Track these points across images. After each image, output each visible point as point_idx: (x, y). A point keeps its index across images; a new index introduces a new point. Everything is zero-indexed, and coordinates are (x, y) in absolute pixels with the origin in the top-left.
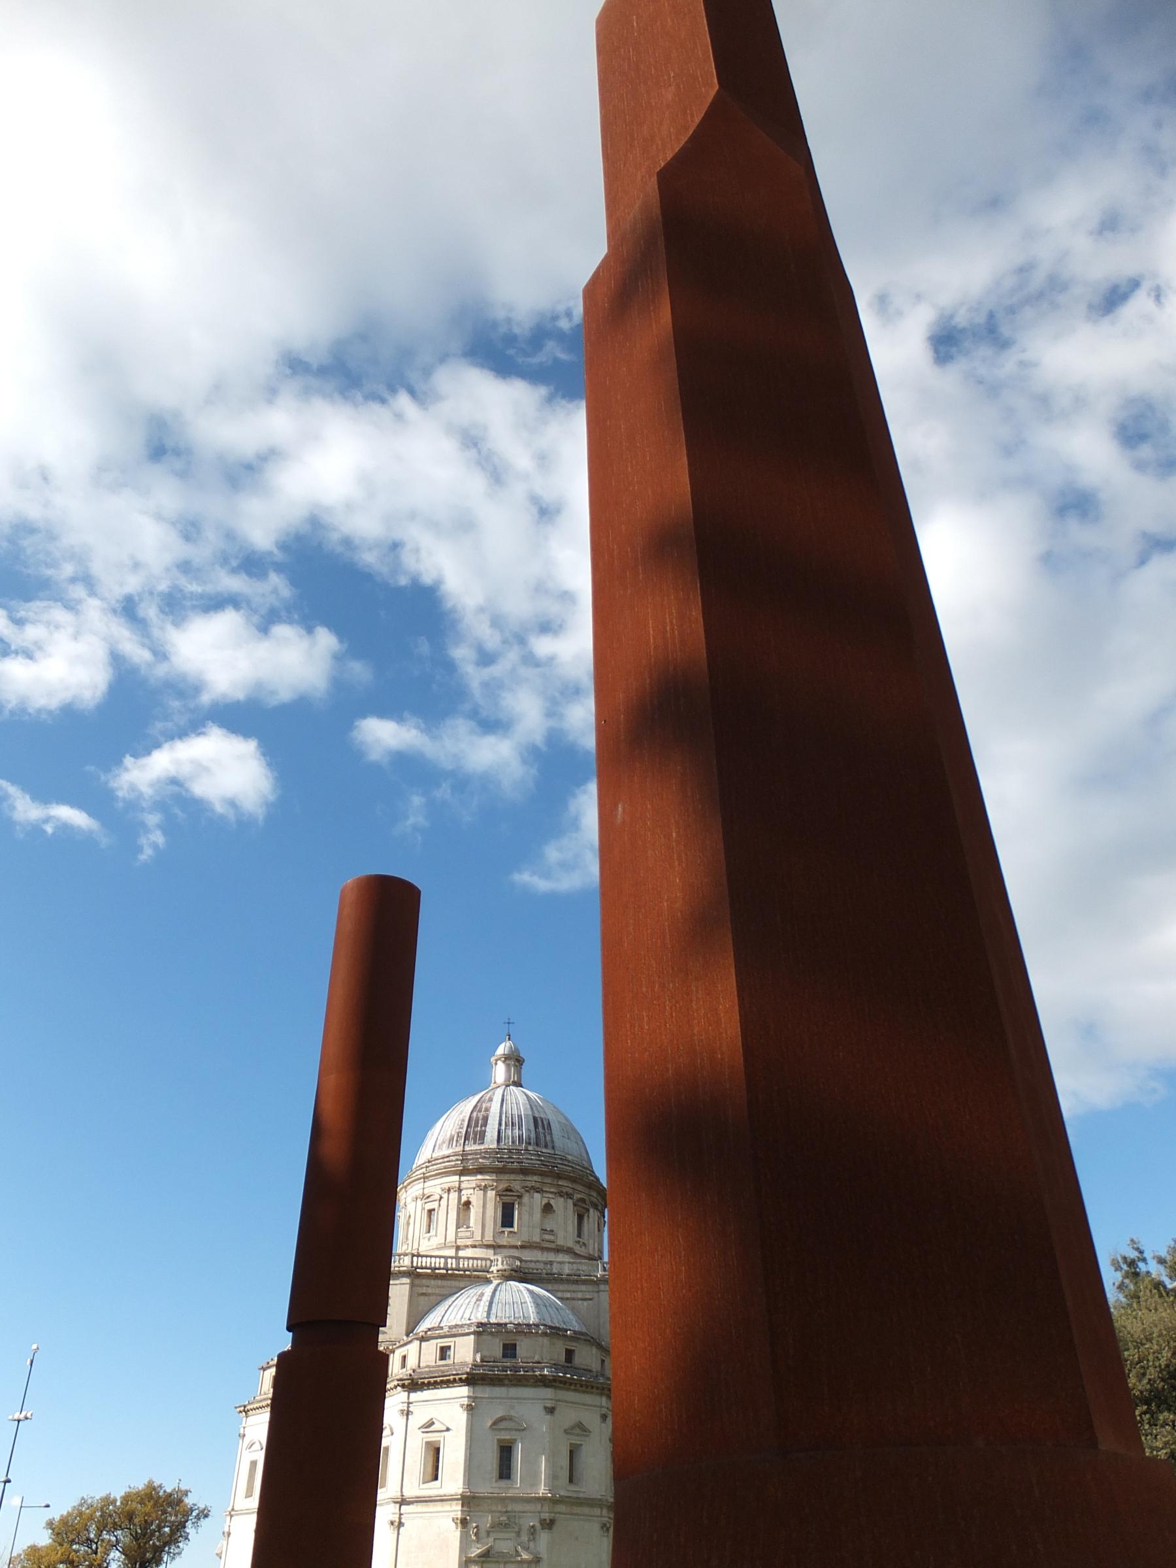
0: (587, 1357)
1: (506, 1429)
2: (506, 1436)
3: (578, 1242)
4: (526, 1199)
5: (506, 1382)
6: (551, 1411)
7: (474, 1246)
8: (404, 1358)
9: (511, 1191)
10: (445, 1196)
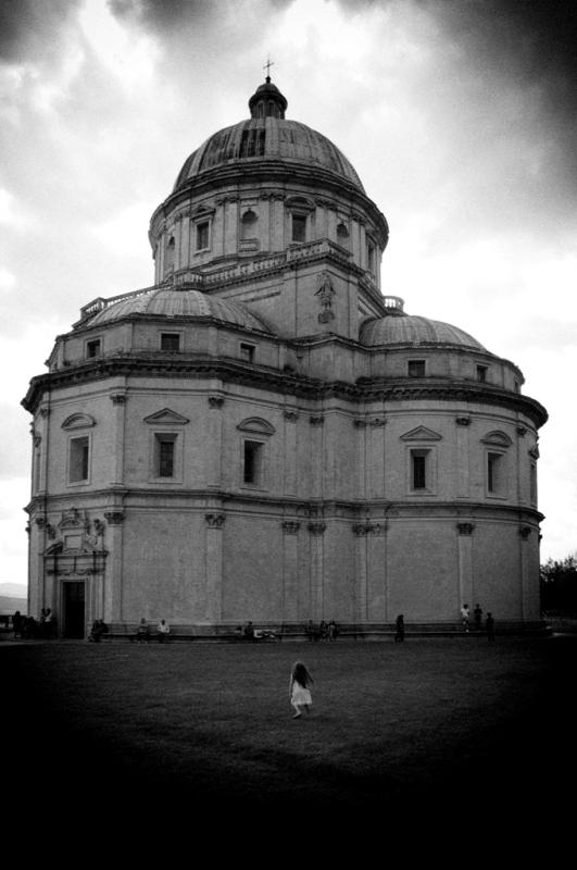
0: (197, 342)
1: (77, 428)
2: (79, 434)
4: (219, 214)
5: (75, 379)
6: (120, 400)
9: (204, 210)
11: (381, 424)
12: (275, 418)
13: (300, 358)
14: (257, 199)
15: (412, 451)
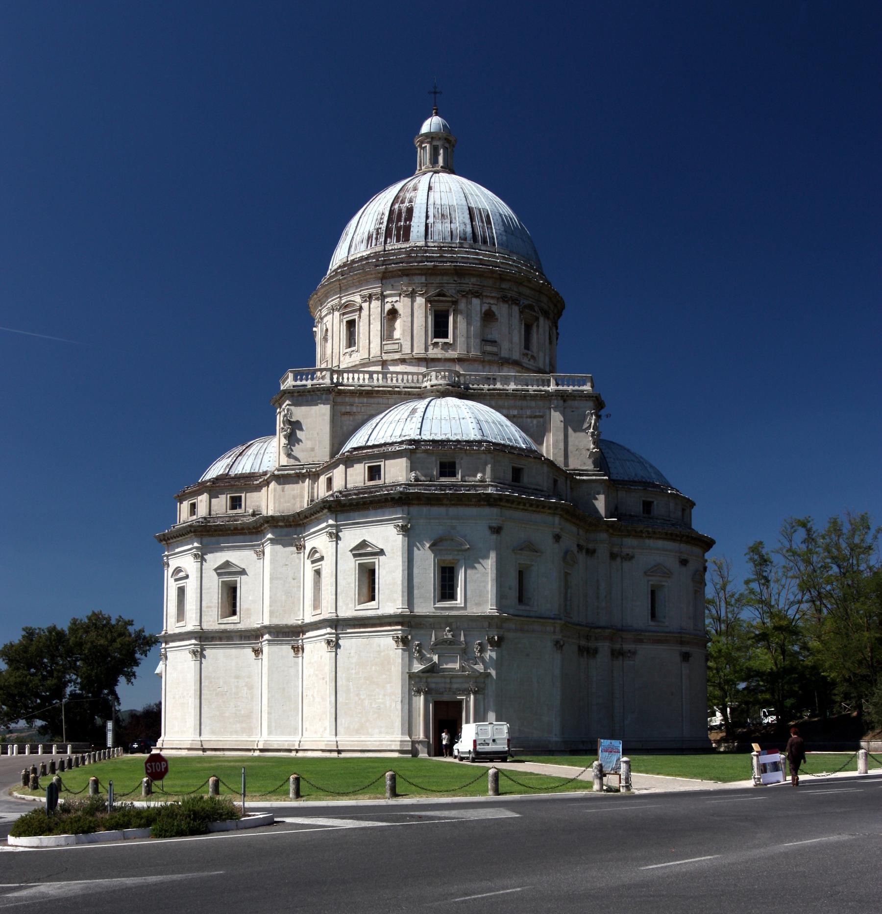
3: (527, 355)
4: (462, 305)
5: (445, 502)
7: (403, 361)
8: (330, 480)
9: (444, 295)
10: (365, 305)
11: (629, 558)
12: (575, 549)
13: (571, 488)
14: (498, 298)
15: (652, 585)
